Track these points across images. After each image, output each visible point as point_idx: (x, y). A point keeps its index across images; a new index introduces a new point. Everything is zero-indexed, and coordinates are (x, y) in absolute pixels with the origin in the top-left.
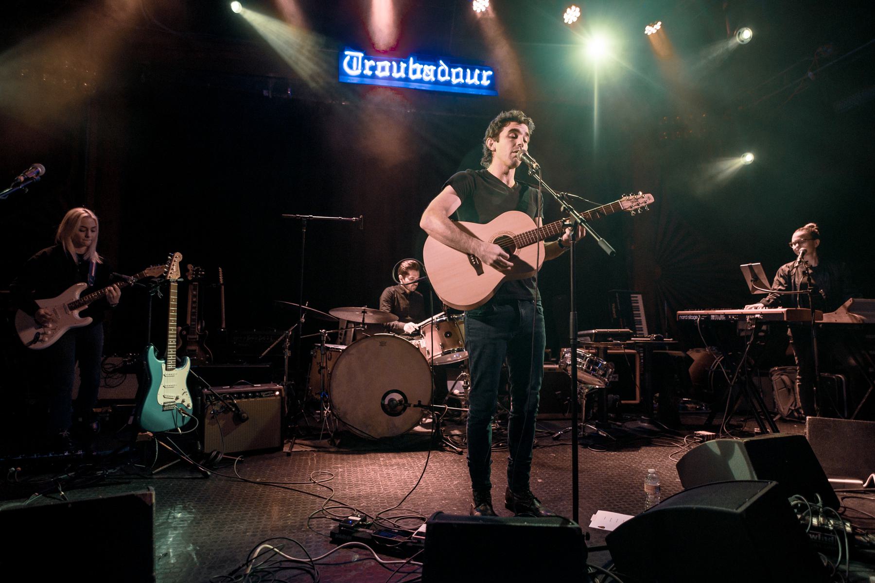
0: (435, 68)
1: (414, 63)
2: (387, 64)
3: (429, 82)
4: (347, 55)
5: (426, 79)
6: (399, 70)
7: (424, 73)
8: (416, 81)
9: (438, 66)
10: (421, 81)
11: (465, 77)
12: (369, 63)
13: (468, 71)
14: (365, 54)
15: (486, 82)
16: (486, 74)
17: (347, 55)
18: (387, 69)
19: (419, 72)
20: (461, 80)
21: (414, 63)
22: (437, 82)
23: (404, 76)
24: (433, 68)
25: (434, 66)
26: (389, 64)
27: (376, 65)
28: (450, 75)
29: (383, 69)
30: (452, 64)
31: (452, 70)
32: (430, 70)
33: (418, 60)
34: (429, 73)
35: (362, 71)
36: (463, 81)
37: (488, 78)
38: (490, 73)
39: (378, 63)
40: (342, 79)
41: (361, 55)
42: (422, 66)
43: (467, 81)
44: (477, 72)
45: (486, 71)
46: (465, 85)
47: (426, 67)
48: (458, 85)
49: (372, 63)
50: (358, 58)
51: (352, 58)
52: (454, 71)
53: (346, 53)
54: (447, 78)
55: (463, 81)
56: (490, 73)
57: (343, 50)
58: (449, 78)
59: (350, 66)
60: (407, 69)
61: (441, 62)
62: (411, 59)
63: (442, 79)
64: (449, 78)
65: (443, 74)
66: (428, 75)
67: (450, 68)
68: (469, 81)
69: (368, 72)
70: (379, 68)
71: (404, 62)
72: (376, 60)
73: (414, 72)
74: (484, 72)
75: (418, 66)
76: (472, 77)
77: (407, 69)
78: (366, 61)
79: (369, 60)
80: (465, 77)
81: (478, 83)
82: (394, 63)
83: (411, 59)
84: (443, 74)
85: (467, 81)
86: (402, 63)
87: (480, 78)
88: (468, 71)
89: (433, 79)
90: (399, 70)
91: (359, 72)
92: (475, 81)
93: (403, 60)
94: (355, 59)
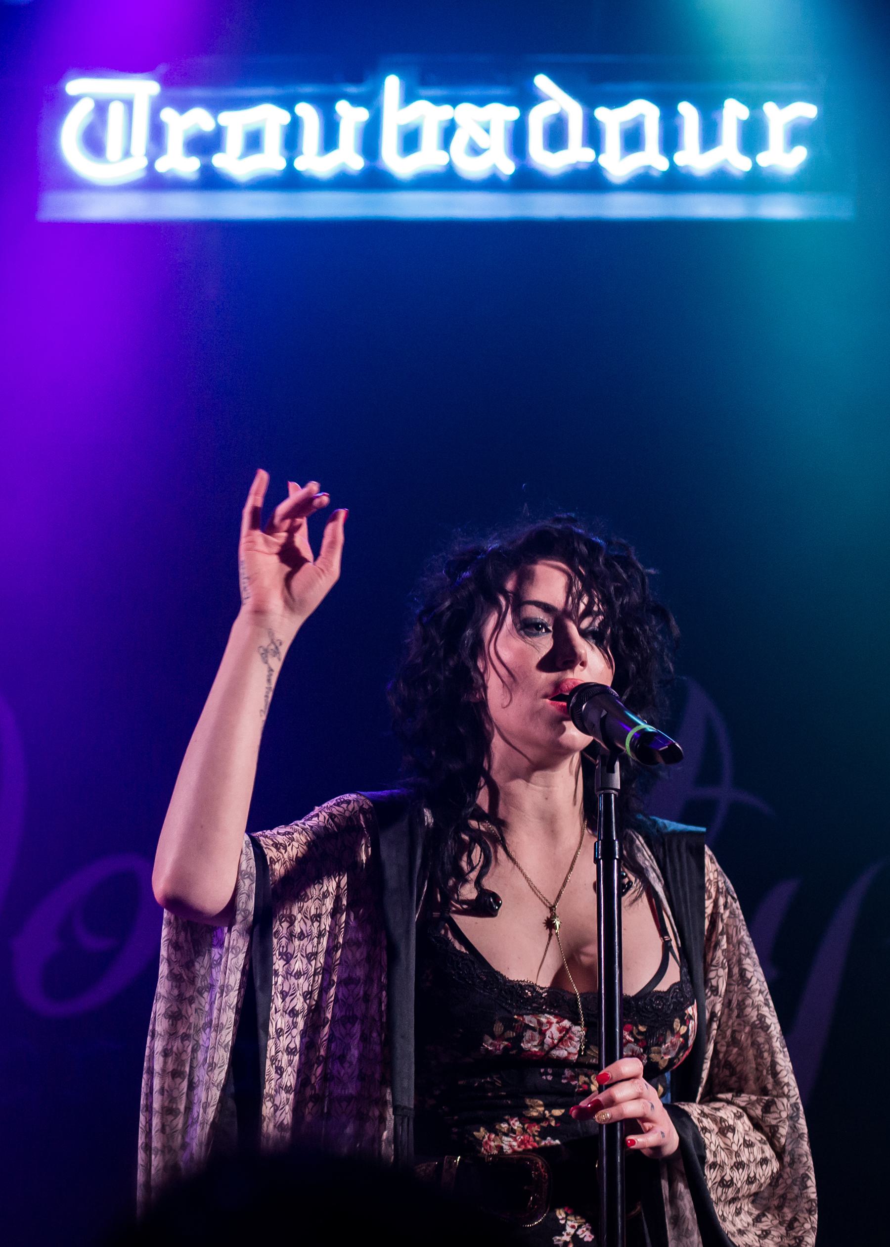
0: (513, 113)
6: (330, 140)
7: (459, 142)
13: (688, 111)
14: (167, 81)
18: (273, 141)
19: (430, 138)
21: (409, 97)
23: (357, 164)
25: (507, 101)
26: (282, 117)
29: (254, 142)
31: (602, 113)
34: (482, 140)
35: (150, 167)
36: (661, 164)
38: (807, 111)
39: (227, 118)
42: (445, 112)
43: (681, 159)
45: (783, 100)
56: (807, 111)
58: (587, 155)
61: (542, 82)
62: (392, 85)
64: (587, 155)
66: (475, 150)
67: (590, 102)
70: (234, 141)
71: (356, 101)
72: (216, 106)
74: (770, 108)
78: (168, 115)
81: (741, 164)
82: (307, 112)
83: (392, 85)
85: (681, 159)
86: (342, 107)
88: (688, 111)
89: (508, 168)
90: (330, 140)
93: (352, 89)
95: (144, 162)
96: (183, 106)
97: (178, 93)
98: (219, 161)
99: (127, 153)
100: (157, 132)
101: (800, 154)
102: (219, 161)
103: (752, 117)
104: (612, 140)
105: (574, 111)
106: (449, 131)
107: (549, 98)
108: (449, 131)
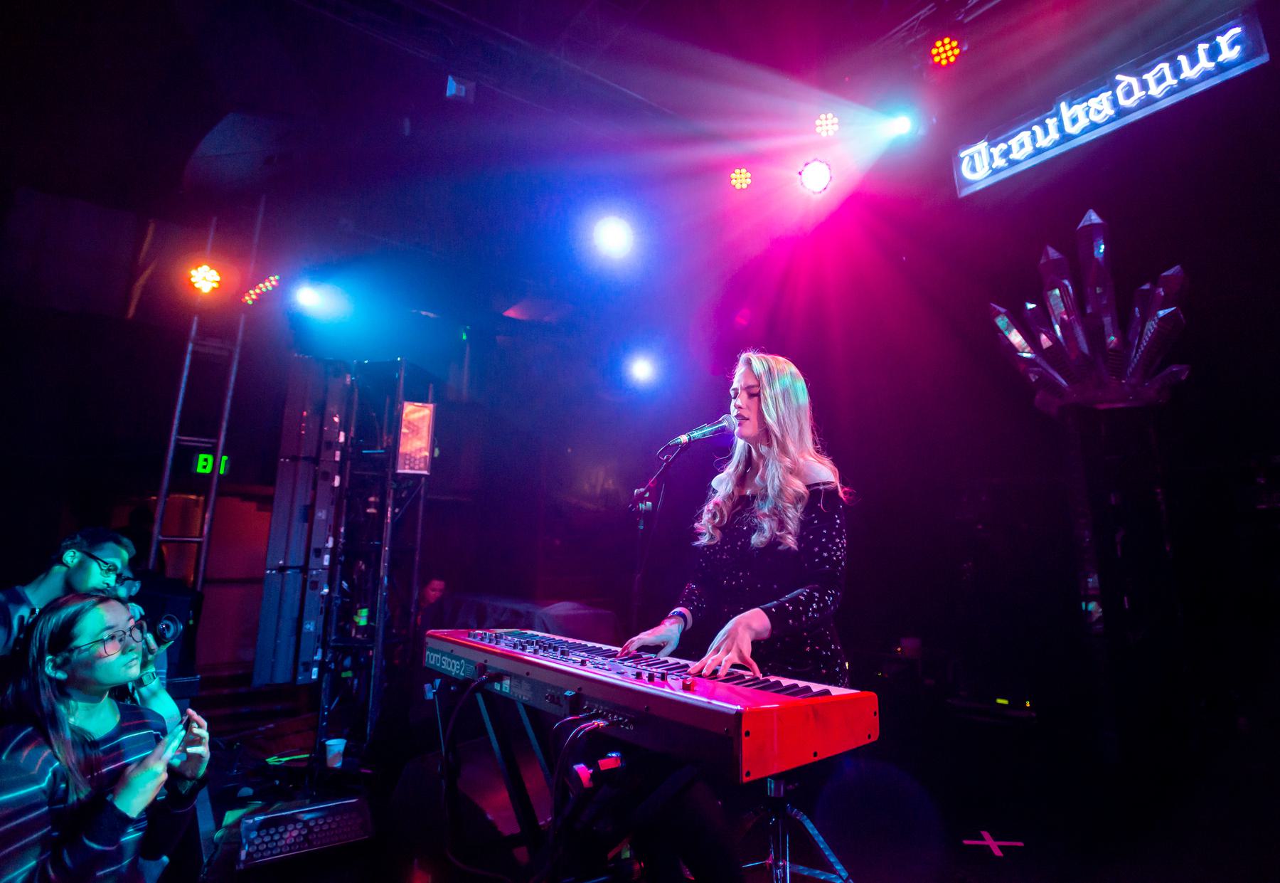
1: (1070, 106)
2: (1025, 136)
3: (1111, 120)
5: (1098, 119)
6: (1046, 133)
7: (1092, 112)
8: (1085, 131)
11: (1177, 71)
12: (996, 151)
13: (1183, 59)
14: (988, 140)
15: (1229, 54)
16: (1223, 41)
20: (1171, 81)
24: (1106, 96)
25: (1107, 91)
26: (1029, 133)
28: (1145, 86)
29: (1022, 145)
30: (1138, 69)
31: (1145, 77)
33: (1073, 98)
34: (1100, 108)
35: (991, 168)
39: (1010, 143)
40: (965, 192)
41: (982, 146)
42: (1085, 104)
44: (1202, 48)
45: (1223, 33)
46: (1184, 85)
47: (1093, 103)
49: (1003, 146)
50: (980, 153)
52: (1150, 77)
53: (962, 155)
54: (1139, 94)
55: (1175, 82)
57: (957, 153)
58: (1144, 93)
59: (973, 169)
60: (1061, 128)
61: (1119, 77)
62: (1063, 106)
65: (1129, 94)
66: (1099, 112)
68: (1188, 73)
69: (1000, 162)
71: (1051, 117)
72: (1005, 141)
73: (1074, 121)
74: (1219, 39)
75: (1078, 109)
76: (1194, 61)
77: (1061, 128)
78: (993, 150)
79: (995, 145)
80: (1177, 71)
81: (1211, 65)
82: (1036, 128)
83: (1063, 106)
84: (1129, 94)
85: (1182, 77)
86: (1048, 121)
87: (1214, 53)
88: (1183, 59)
89: (1112, 112)
90: (1046, 133)
92: (1205, 64)
93: (1049, 113)
94: (976, 156)
95: (987, 168)
97: (993, 141)
98: (1011, 157)
100: (991, 156)
101: (1238, 48)
102: (1011, 157)
103: (1211, 47)
104: (1152, 83)
105: (1134, 81)
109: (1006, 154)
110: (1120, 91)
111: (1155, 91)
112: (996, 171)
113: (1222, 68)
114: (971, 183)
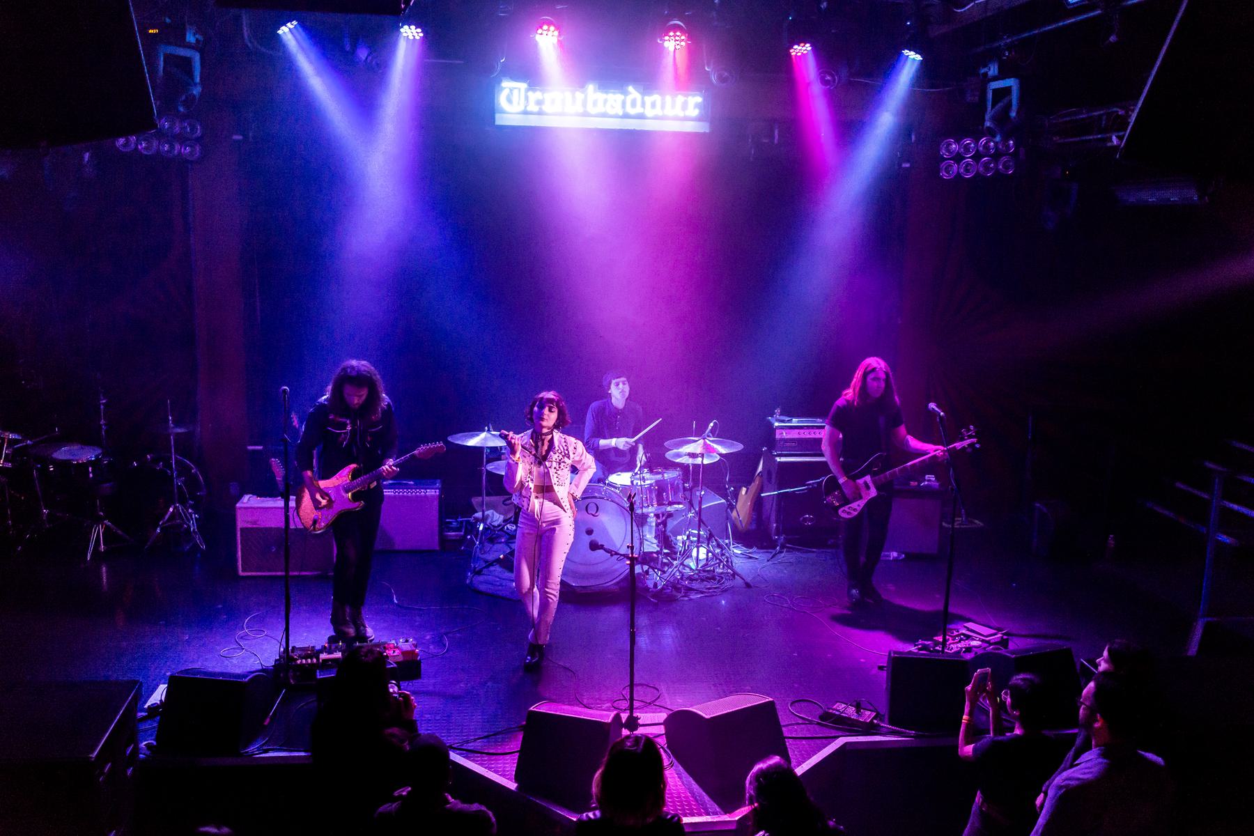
1: (595, 91)
4: (505, 88)
9: (626, 93)
10: (604, 115)
11: (663, 107)
12: (534, 96)
14: (530, 85)
15: (694, 113)
17: (505, 88)
19: (600, 103)
22: (626, 116)
23: (581, 110)
25: (622, 93)
27: (544, 98)
28: (643, 104)
32: (615, 101)
35: (526, 107)
37: (697, 106)
41: (523, 86)
45: (694, 96)
48: (656, 118)
50: (520, 89)
51: (511, 90)
52: (648, 99)
54: (638, 110)
59: (509, 101)
60: (584, 104)
61: (630, 88)
63: (632, 111)
65: (634, 104)
66: (612, 107)
68: (669, 112)
69: (533, 107)
71: (583, 92)
72: (543, 91)
73: (595, 103)
75: (601, 96)
76: (673, 106)
77: (584, 104)
78: (530, 94)
80: (663, 107)
81: (681, 114)
82: (568, 95)
84: (634, 104)
87: (685, 106)
89: (621, 113)
91: (521, 108)
96: (534, 91)
99: (519, 103)
106: (605, 101)
107: (630, 93)
108: (605, 101)
109: (539, 103)
110: (629, 98)
111: (649, 112)
112: (525, 113)
113: (686, 119)
114: (503, 112)
